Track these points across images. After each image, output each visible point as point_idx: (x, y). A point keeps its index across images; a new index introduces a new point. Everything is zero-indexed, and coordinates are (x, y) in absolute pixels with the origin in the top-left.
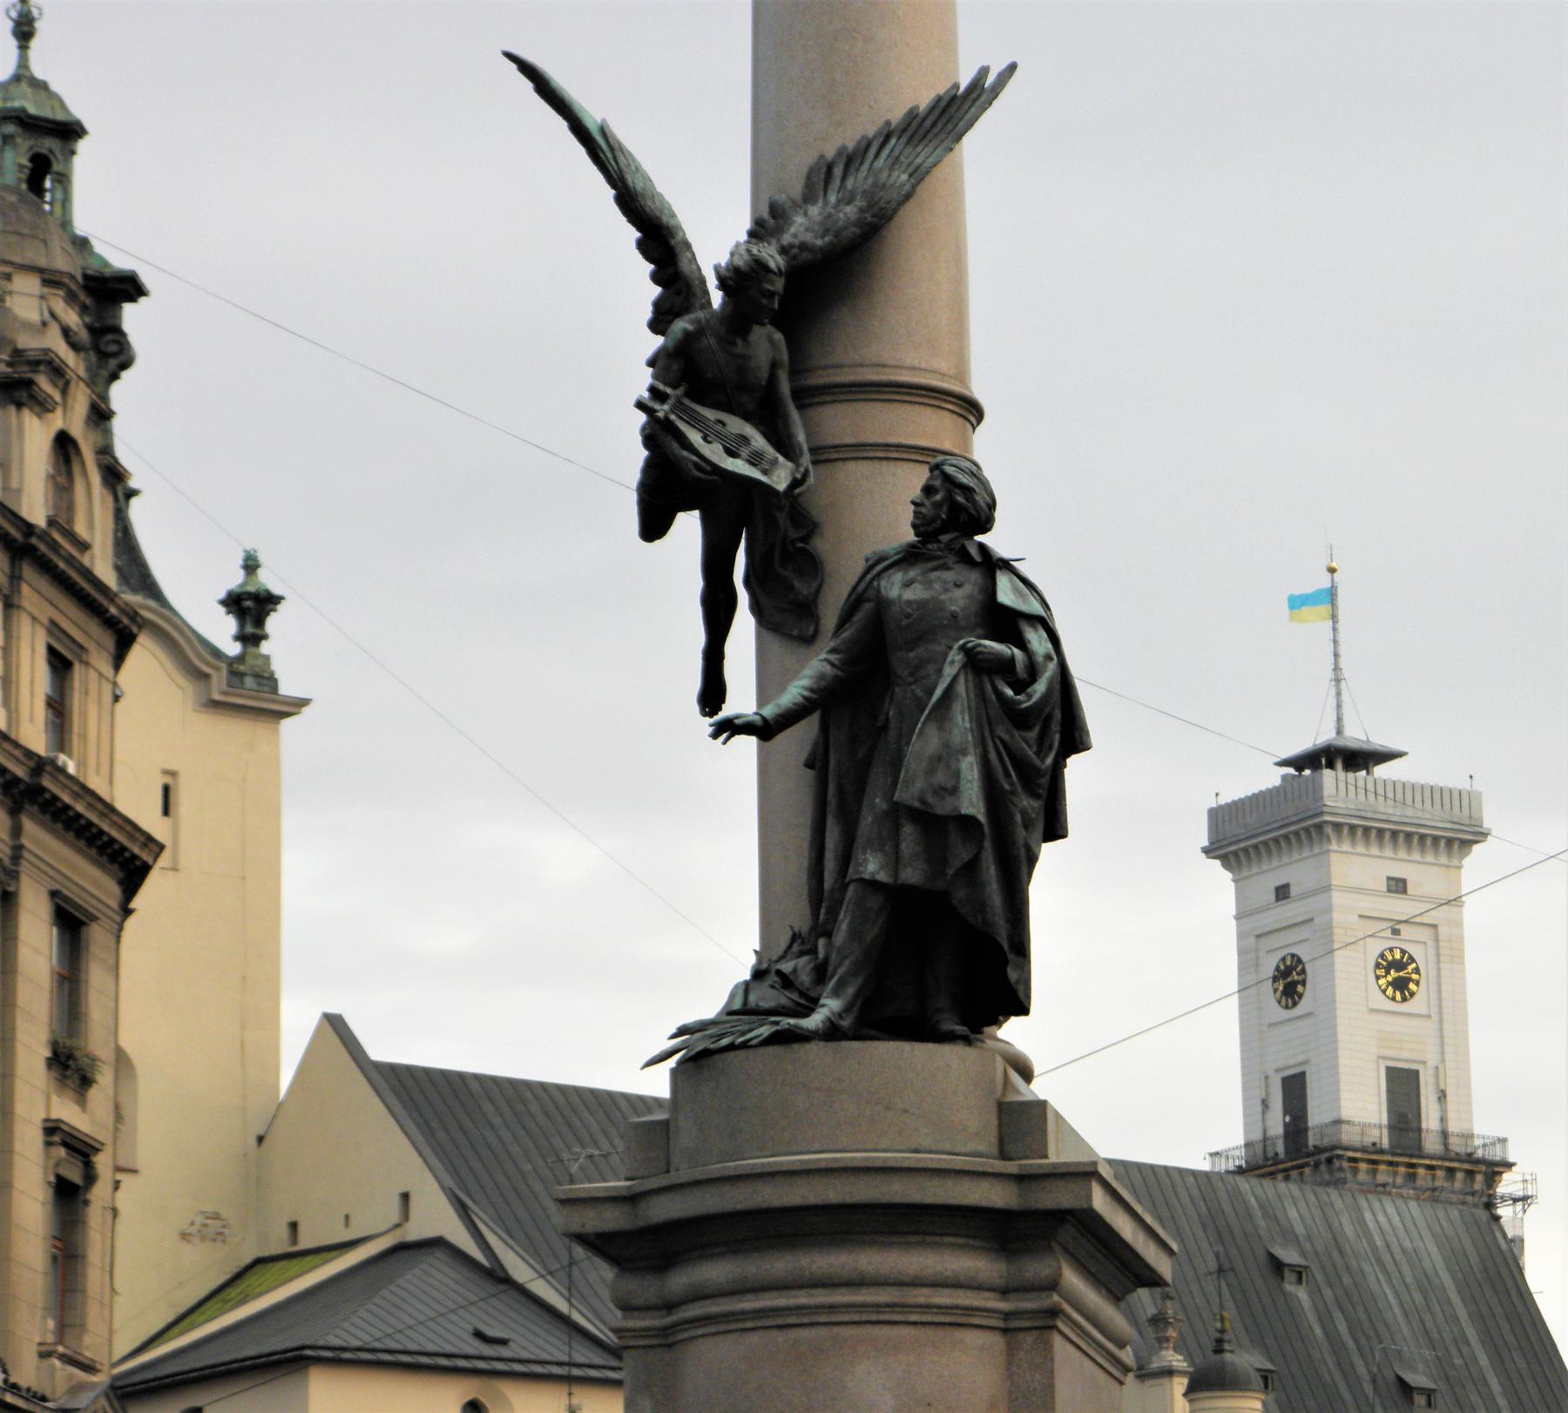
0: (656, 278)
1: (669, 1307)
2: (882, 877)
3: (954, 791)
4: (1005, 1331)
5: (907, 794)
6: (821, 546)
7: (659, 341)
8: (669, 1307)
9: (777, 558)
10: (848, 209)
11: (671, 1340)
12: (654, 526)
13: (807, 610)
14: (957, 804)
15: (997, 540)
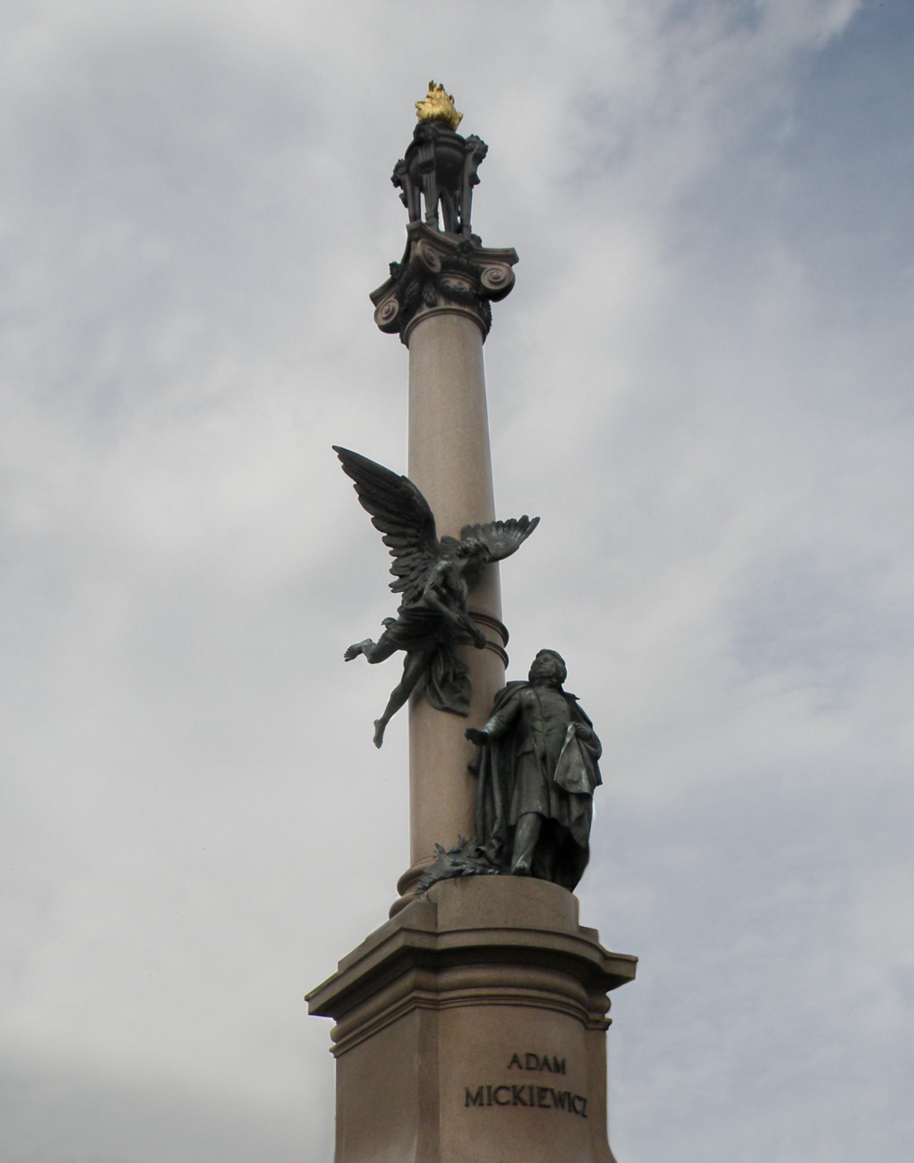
0: (391, 553)
1: (437, 991)
2: (546, 814)
3: (577, 783)
4: (586, 1028)
5: (558, 777)
6: (470, 677)
7: (397, 578)
8: (437, 991)
9: (451, 678)
10: (498, 543)
11: (441, 1007)
12: (378, 654)
13: (465, 701)
14: (579, 788)
15: (566, 687)
